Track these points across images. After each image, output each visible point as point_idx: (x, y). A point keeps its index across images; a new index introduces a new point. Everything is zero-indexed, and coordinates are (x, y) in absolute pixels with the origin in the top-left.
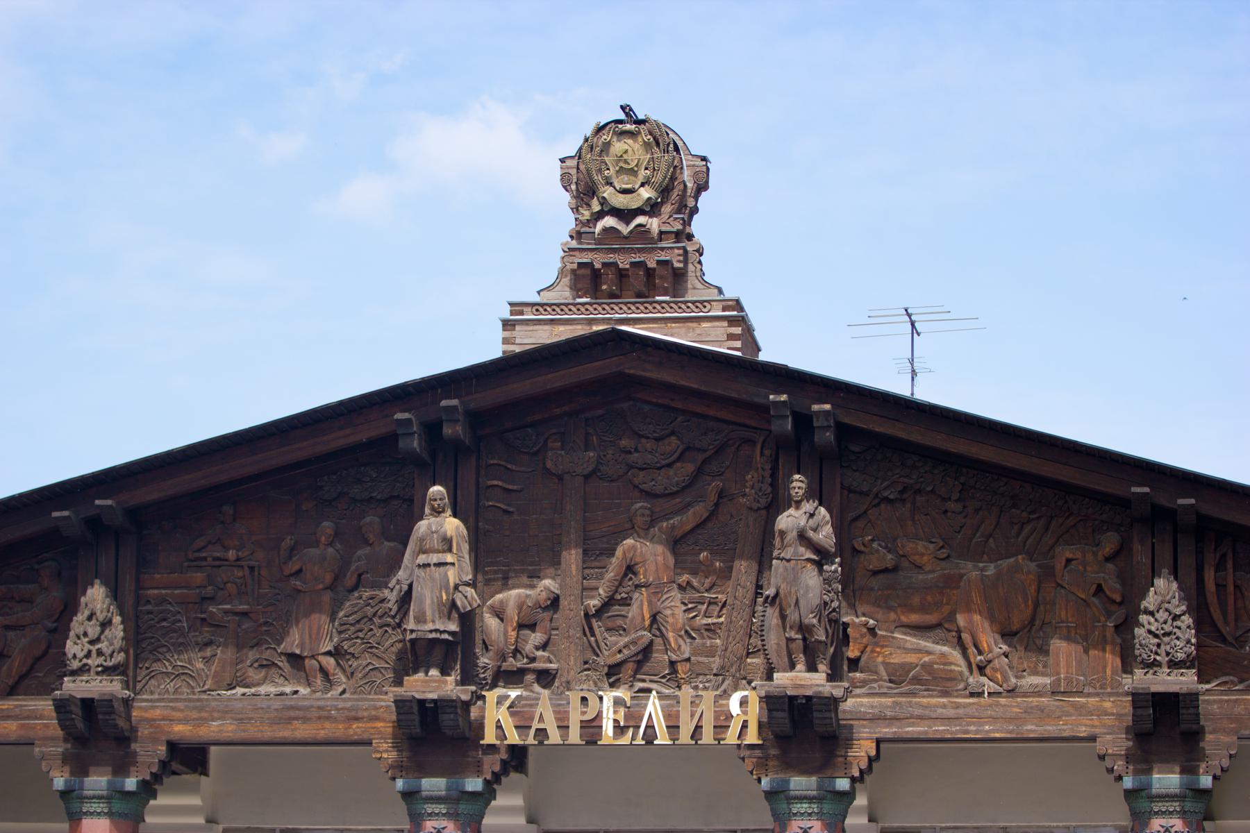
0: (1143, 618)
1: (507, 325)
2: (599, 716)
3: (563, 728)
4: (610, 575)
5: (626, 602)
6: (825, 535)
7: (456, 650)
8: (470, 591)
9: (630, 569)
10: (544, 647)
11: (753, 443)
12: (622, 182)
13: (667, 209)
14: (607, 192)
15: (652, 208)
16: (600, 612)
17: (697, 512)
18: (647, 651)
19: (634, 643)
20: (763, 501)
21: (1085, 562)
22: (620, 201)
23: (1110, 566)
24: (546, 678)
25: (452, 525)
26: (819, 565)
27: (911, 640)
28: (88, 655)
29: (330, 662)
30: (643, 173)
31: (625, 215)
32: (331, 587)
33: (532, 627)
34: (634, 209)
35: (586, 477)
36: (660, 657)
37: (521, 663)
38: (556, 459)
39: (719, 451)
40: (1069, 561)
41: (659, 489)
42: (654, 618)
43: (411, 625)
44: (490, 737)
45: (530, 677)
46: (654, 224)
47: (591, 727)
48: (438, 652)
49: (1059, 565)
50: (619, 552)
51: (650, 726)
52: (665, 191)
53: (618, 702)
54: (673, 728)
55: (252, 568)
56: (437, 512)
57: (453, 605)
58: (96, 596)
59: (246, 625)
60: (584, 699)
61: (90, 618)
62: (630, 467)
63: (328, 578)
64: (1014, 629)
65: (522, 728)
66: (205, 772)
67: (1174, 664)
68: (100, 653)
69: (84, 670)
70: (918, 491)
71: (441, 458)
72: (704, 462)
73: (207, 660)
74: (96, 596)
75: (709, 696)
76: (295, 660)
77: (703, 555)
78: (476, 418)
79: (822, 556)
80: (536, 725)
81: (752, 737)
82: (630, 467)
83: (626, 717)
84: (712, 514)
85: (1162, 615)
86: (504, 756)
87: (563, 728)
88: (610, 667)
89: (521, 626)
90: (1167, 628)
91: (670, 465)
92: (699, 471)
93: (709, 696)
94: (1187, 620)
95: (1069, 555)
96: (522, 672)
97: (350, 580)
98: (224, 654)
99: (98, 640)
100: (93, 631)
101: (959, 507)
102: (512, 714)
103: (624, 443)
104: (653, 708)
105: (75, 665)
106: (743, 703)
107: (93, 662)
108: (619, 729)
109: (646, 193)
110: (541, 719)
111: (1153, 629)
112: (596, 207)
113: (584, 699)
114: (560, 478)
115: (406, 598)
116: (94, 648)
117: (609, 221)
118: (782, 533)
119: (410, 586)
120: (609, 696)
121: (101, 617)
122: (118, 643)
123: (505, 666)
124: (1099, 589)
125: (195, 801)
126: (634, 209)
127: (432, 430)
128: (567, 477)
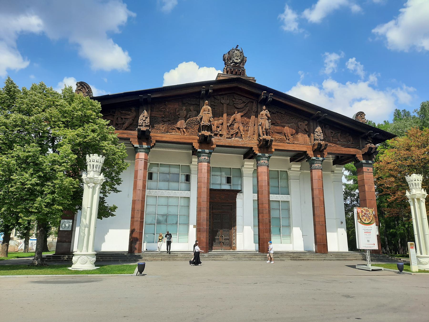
0: (316, 133)
1: (218, 76)
4: (231, 120)
5: (233, 125)
7: (209, 128)
9: (234, 120)
11: (253, 102)
14: (234, 59)
15: (240, 63)
16: (230, 126)
21: (303, 125)
22: (236, 61)
26: (268, 120)
31: (236, 63)
33: (218, 127)
34: (234, 64)
36: (239, 134)
45: (218, 135)
48: (207, 128)
49: (299, 125)
52: (242, 61)
62: (234, 103)
63: (185, 116)
68: (145, 123)
69: (142, 125)
70: (278, 112)
71: (207, 96)
73: (163, 127)
76: (179, 129)
78: (214, 91)
79: (268, 118)
82: (234, 103)
85: (319, 133)
89: (217, 127)
94: (322, 134)
96: (217, 134)
98: (165, 126)
100: (144, 119)
103: (233, 100)
105: (140, 124)
107: (144, 124)
109: (239, 60)
114: (223, 104)
115: (201, 119)
126: (234, 64)
127: (207, 91)
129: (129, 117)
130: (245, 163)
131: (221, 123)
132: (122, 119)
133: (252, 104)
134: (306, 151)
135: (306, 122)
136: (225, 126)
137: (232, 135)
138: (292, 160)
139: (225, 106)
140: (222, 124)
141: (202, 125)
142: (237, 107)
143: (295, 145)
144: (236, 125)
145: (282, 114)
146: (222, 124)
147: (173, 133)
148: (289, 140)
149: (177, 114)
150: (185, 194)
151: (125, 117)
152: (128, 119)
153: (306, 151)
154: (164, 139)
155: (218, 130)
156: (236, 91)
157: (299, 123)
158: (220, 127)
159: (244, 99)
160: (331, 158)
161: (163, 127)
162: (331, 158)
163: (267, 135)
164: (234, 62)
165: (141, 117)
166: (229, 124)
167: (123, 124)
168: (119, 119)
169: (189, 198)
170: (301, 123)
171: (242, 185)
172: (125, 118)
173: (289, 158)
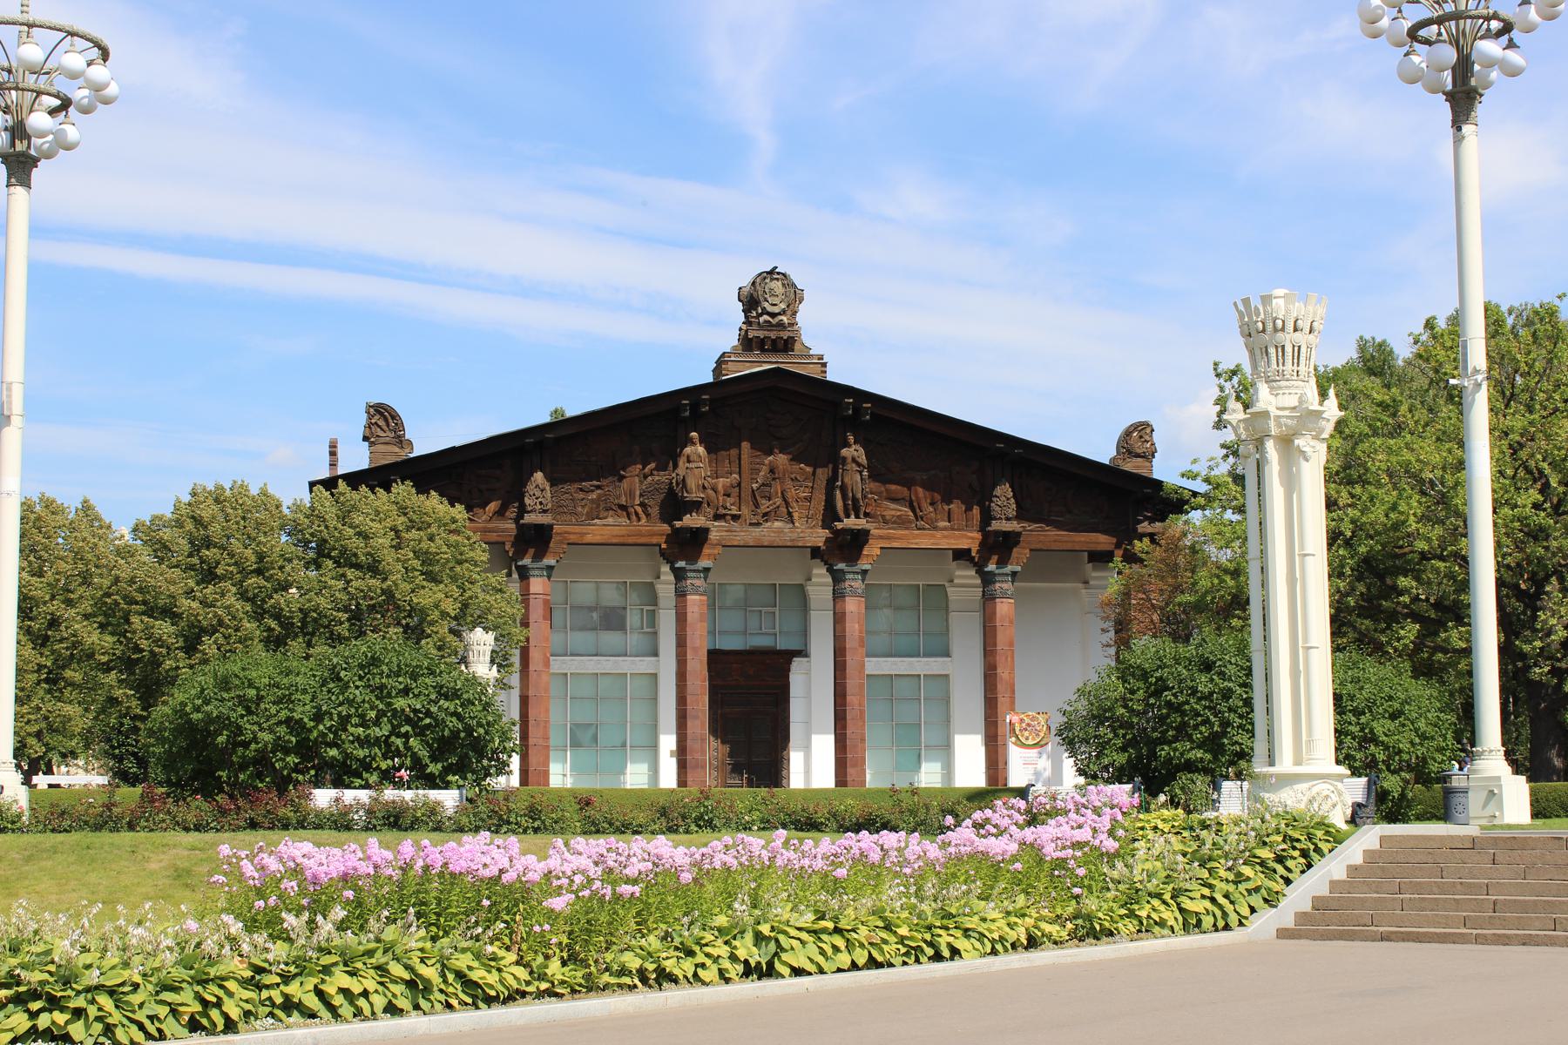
6: (863, 460)
14: (766, 305)
15: (783, 312)
22: (770, 309)
25: (701, 450)
27: (893, 506)
31: (773, 315)
46: (784, 318)
56: (694, 444)
58: (539, 476)
67: (1008, 519)
71: (696, 421)
74: (539, 476)
76: (623, 508)
109: (783, 306)
117: (766, 317)
118: (844, 459)
130: (815, 571)
137: (765, 514)
143: (939, 534)
147: (610, 520)
150: (644, 665)
154: (589, 538)
156: (774, 405)
163: (857, 517)
165: (530, 488)
169: (655, 676)
171: (805, 633)
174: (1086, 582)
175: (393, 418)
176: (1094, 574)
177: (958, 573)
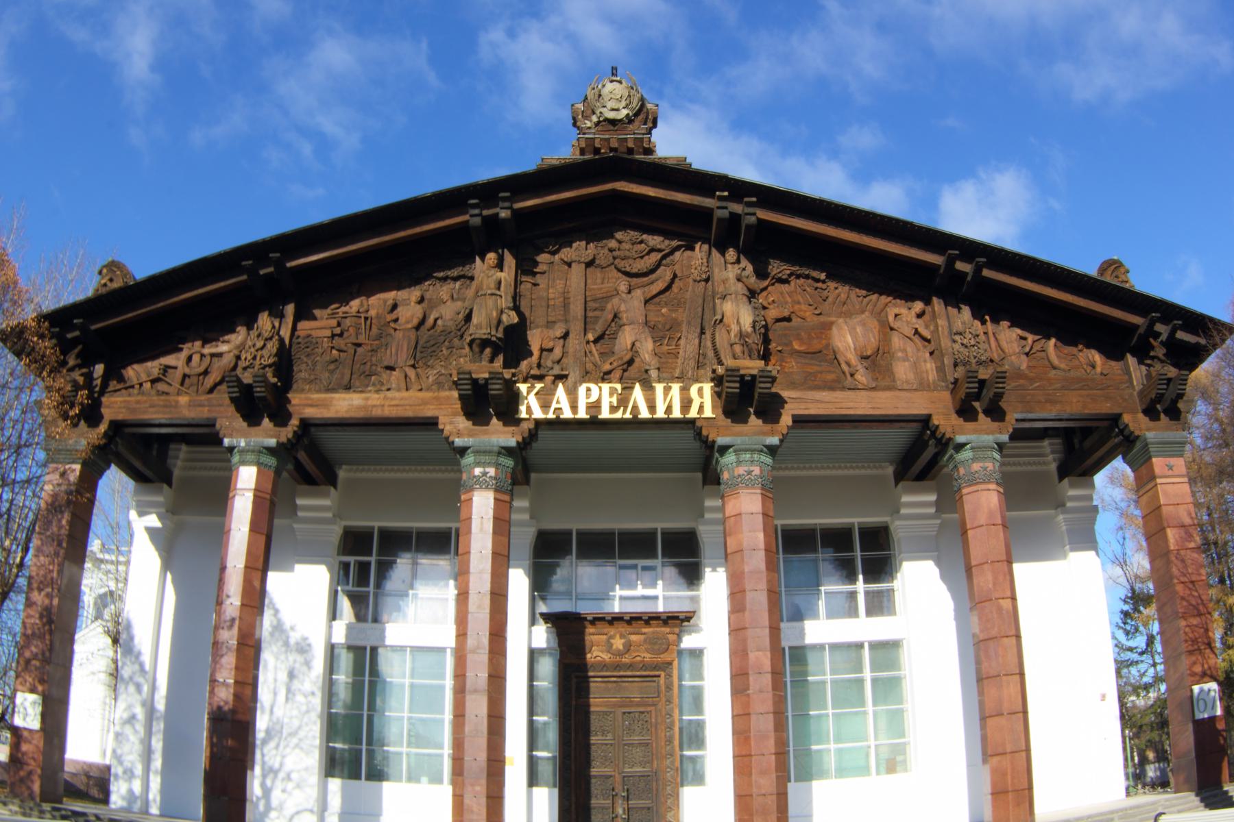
2: (599, 401)
3: (574, 408)
4: (601, 322)
5: (614, 337)
8: (513, 314)
10: (558, 362)
12: (610, 105)
13: (637, 123)
14: (603, 110)
17: (660, 286)
18: (630, 362)
19: (621, 358)
20: (704, 276)
22: (611, 115)
23: (920, 321)
24: (561, 377)
28: (254, 358)
29: (411, 373)
30: (623, 104)
31: (613, 122)
32: (417, 328)
33: (551, 350)
35: (589, 264)
37: (543, 371)
38: (566, 253)
39: (672, 252)
40: (896, 315)
41: (635, 271)
42: (633, 344)
43: (471, 330)
44: (523, 415)
45: (549, 379)
47: (595, 406)
49: (891, 318)
50: (609, 306)
51: (635, 407)
53: (612, 392)
54: (652, 408)
55: (366, 319)
57: (499, 322)
59: (360, 350)
60: (589, 390)
61: (259, 336)
63: (415, 322)
64: (869, 353)
65: (545, 406)
66: (335, 486)
70: (798, 277)
72: (664, 257)
73: (332, 372)
75: (676, 388)
77: (664, 310)
79: (752, 294)
80: (554, 405)
81: (708, 413)
82: (614, 258)
83: (619, 401)
84: (668, 288)
86: (532, 426)
87: (574, 408)
88: (606, 373)
89: (542, 350)
90: (973, 342)
91: (642, 257)
92: (658, 265)
93: (676, 388)
95: (896, 310)
97: (430, 321)
99: (262, 348)
100: (260, 344)
101: (824, 286)
102: (538, 399)
104: (638, 393)
106: (700, 390)
108: (613, 409)
109: (625, 112)
110: (558, 402)
111: (965, 341)
112: (595, 119)
113: (589, 390)
114: (569, 265)
116: (260, 353)
119: (471, 311)
120: (606, 387)
121: (266, 335)
122: (275, 350)
123: (532, 372)
124: (916, 332)
125: (326, 502)
128: (573, 265)
129: (223, 348)
131: (559, 333)
132: (203, 356)
133: (688, 253)
134: (929, 417)
135: (918, 306)
136: (574, 342)
137: (609, 372)
138: (899, 477)
139: (577, 269)
140: (565, 336)
141: (469, 339)
142: (628, 269)
144: (626, 337)
145: (817, 281)
146: (565, 336)
148: (852, 375)
149: (390, 317)
151: (214, 350)
152: (220, 355)
153: (929, 417)
155: (549, 364)
157: (892, 311)
158: (558, 352)
159: (655, 241)
160: (1051, 457)
161: (332, 372)
162: (1051, 457)
164: (606, 120)
166: (591, 337)
167: (206, 373)
168: (196, 358)
170: (896, 310)
172: (213, 355)
173: (890, 470)
174: (1063, 505)
175: (119, 268)
176: (1072, 492)
177: (905, 499)
